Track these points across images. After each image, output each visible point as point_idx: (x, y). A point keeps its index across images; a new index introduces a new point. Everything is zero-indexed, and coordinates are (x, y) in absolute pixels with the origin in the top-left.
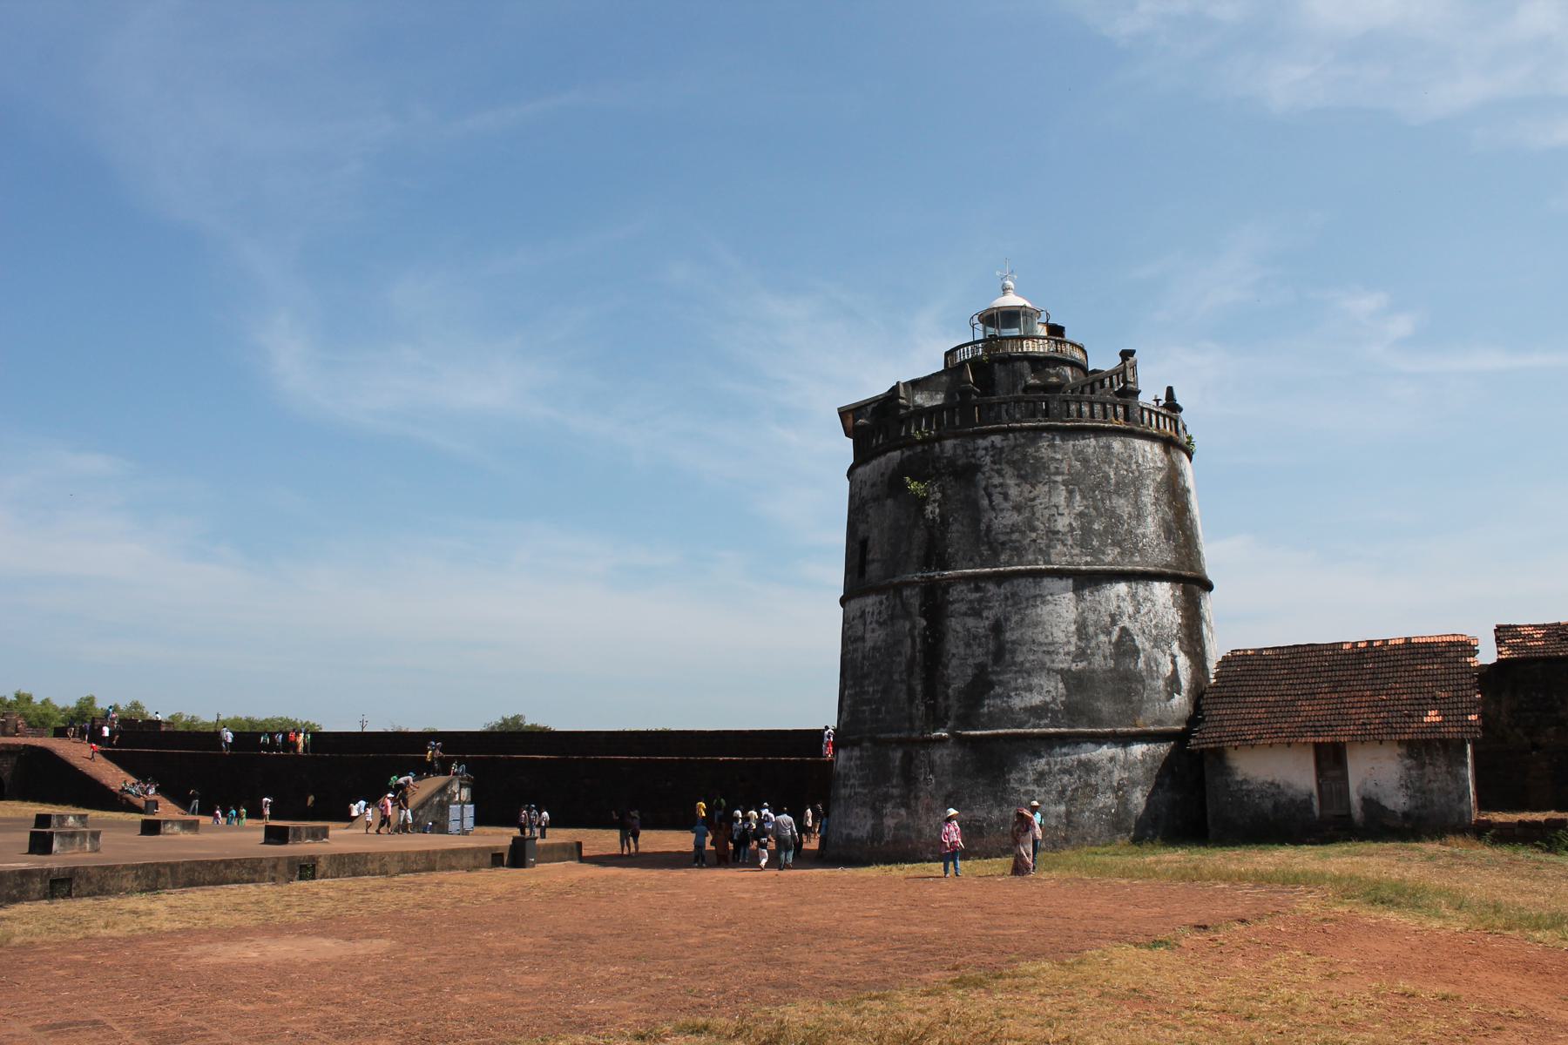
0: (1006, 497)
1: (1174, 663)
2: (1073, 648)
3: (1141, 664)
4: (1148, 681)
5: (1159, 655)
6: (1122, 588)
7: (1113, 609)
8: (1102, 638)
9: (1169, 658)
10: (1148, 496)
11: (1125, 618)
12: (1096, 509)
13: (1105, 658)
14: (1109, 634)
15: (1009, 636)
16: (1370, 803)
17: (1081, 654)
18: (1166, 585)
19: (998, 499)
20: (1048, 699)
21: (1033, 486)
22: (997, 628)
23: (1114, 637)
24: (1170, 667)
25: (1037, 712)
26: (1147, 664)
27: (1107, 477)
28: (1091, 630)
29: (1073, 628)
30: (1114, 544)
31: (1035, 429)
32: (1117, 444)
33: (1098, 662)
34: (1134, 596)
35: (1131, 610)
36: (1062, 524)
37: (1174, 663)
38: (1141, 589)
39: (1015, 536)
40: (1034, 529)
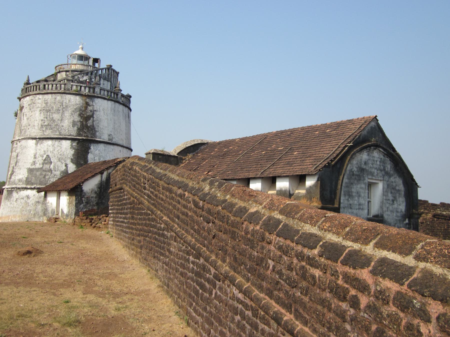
0: (26, 115)
1: (66, 165)
2: (31, 161)
3: (52, 166)
4: (53, 172)
5: (59, 163)
6: (50, 142)
7: (45, 149)
8: (40, 158)
9: (64, 165)
10: (67, 114)
11: (49, 152)
12: (46, 118)
13: (40, 164)
14: (43, 157)
15: (19, 158)
16: (62, 212)
17: (34, 163)
18: (69, 142)
19: (25, 116)
20: (23, 176)
21: (32, 112)
22: (17, 156)
23: (44, 158)
24: (64, 168)
25: (20, 180)
26: (54, 167)
27: (52, 108)
28: (37, 156)
29: (33, 155)
30: (50, 129)
31: (35, 94)
32: (59, 97)
33: (38, 166)
34: (53, 146)
35: (51, 150)
36: (36, 124)
37: (66, 165)
38: (57, 143)
39: (25, 128)
40: (29, 125)
